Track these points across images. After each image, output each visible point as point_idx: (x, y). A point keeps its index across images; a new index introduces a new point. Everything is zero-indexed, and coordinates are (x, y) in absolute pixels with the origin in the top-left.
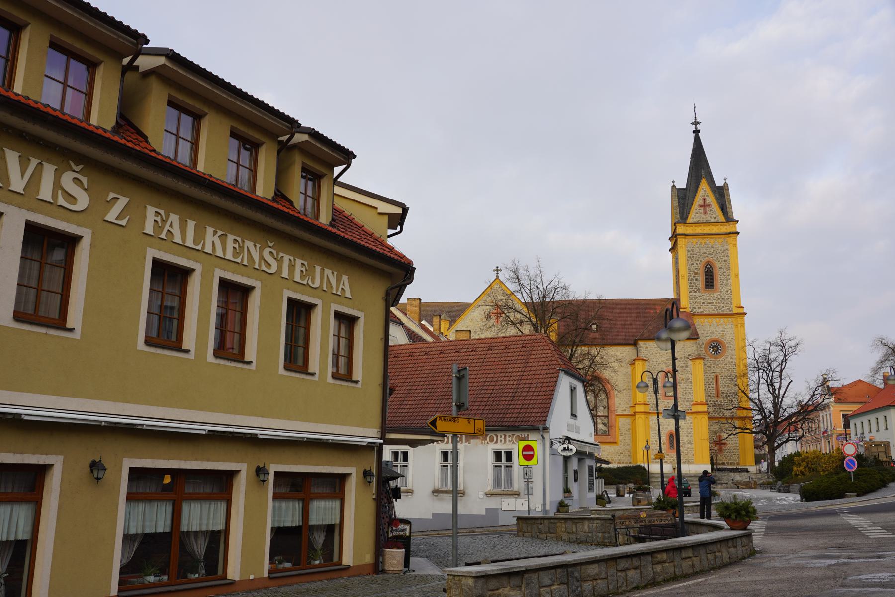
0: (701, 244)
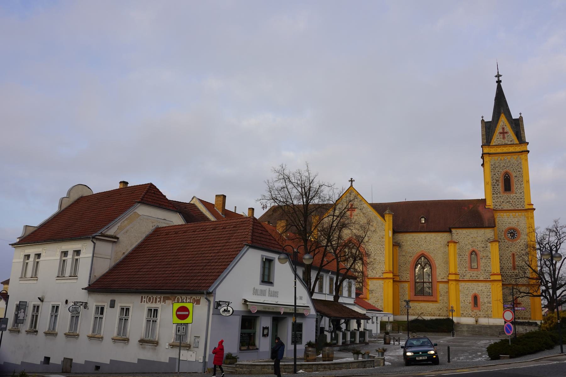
0: (501, 160)
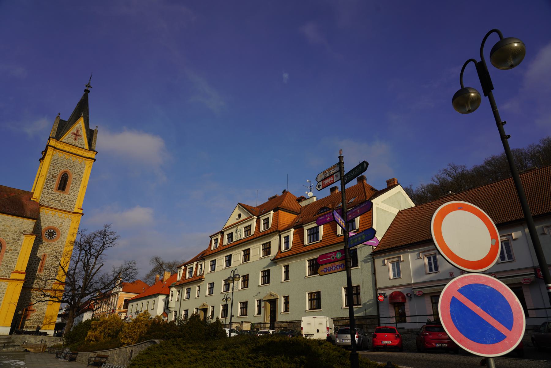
0: (65, 158)
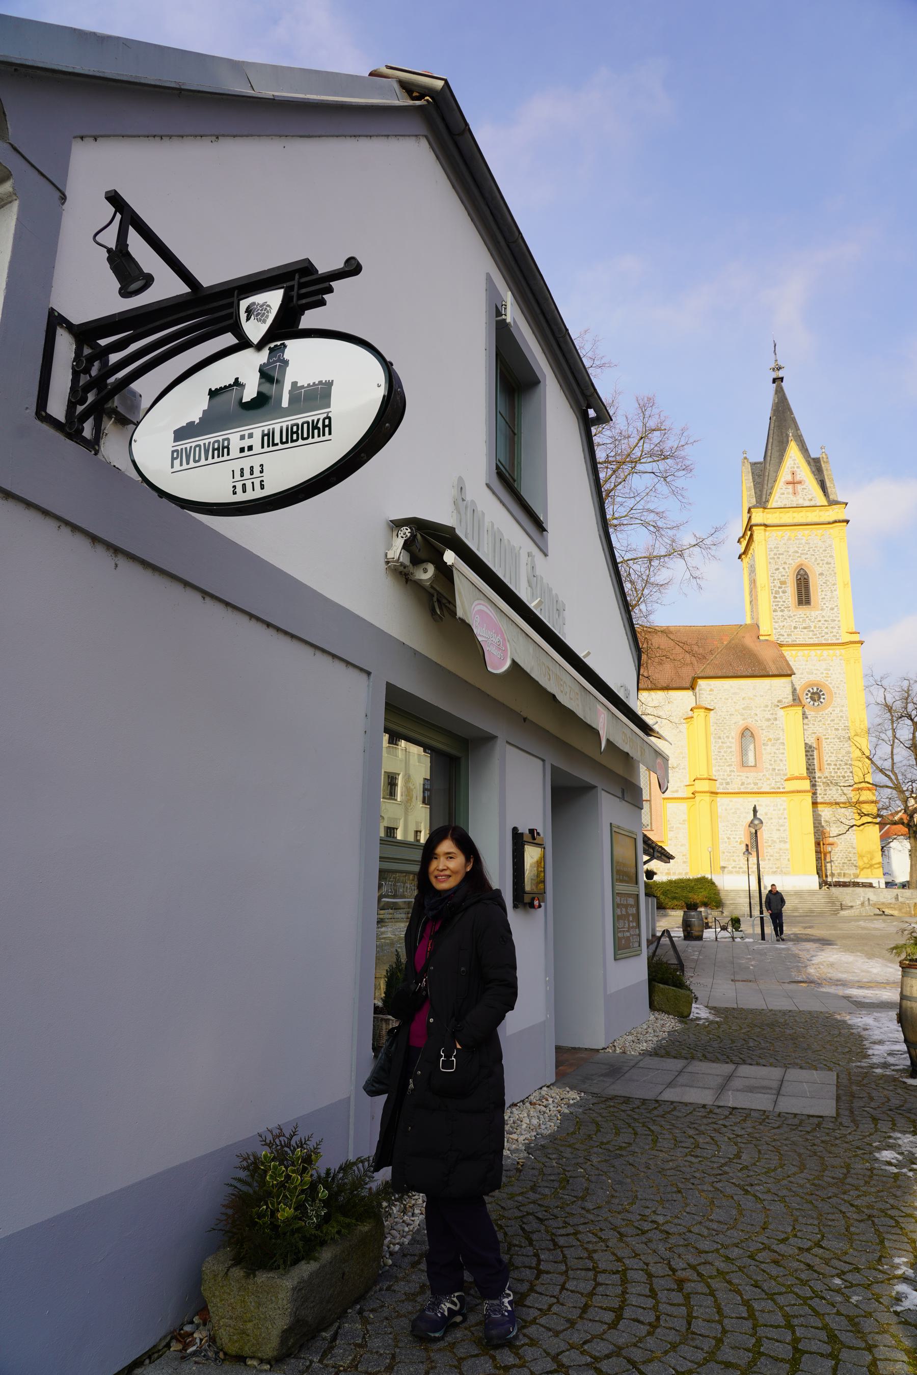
0: (789, 539)
